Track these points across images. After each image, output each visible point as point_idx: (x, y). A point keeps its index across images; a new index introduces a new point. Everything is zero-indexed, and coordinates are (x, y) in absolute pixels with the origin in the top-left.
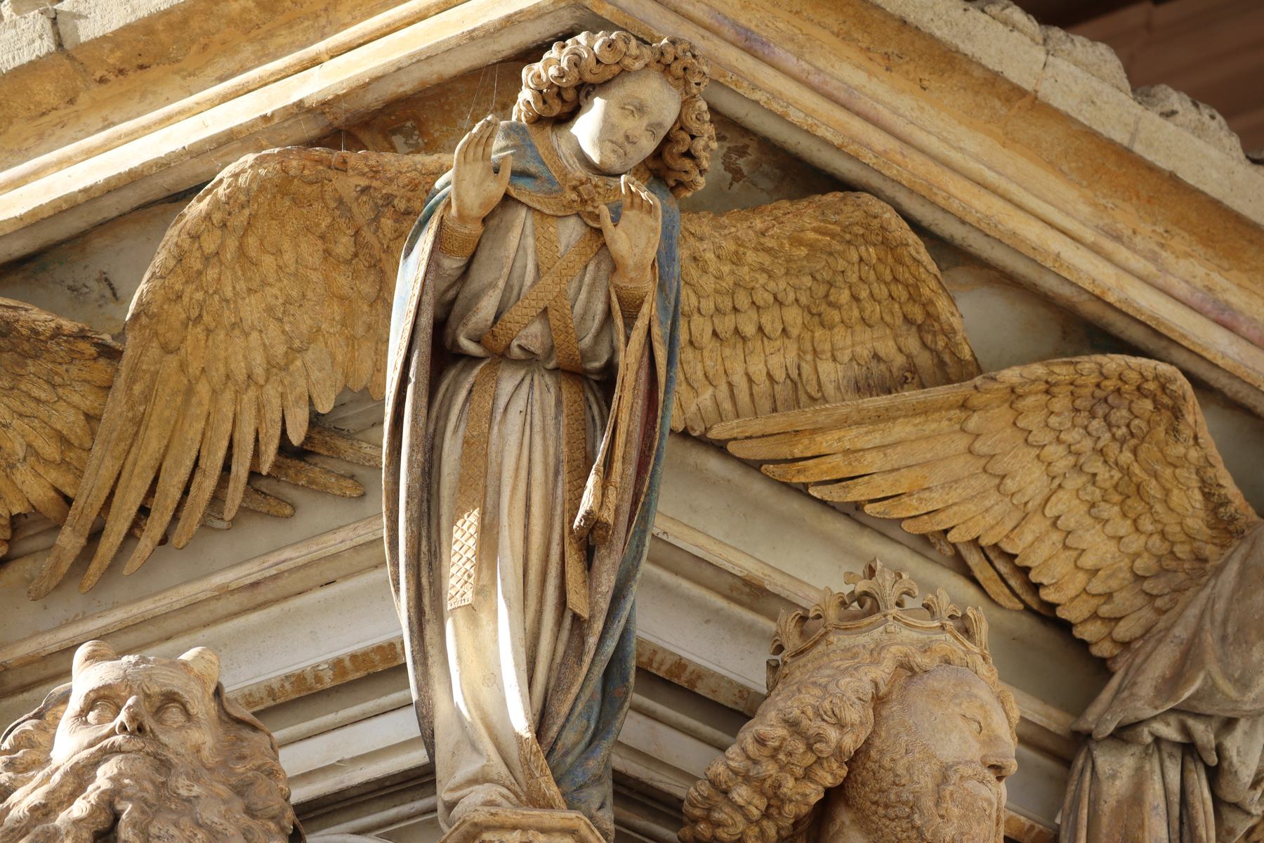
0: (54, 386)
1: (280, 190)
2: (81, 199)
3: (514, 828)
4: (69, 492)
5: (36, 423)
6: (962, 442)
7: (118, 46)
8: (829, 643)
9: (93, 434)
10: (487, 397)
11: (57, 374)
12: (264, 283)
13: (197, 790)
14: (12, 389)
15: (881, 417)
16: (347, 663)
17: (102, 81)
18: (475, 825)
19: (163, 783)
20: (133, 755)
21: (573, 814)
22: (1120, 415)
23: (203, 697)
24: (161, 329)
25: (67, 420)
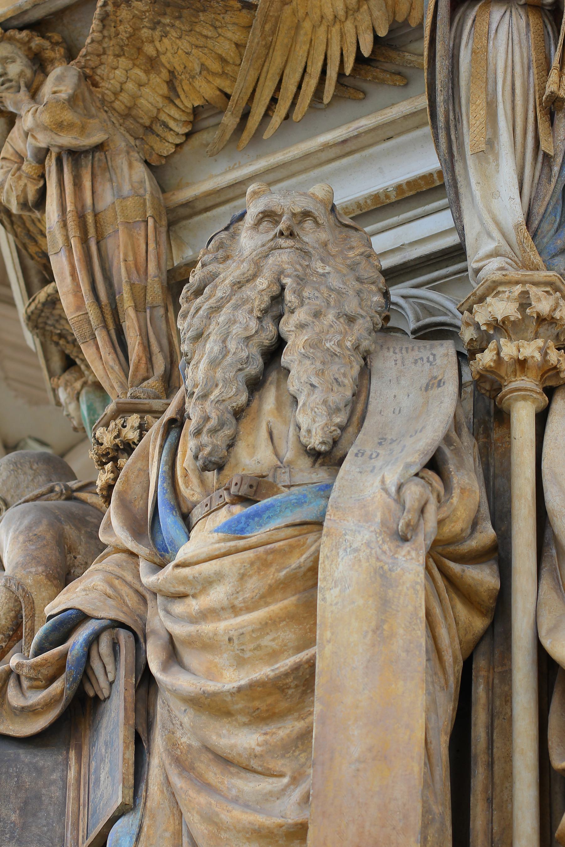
0: (216, 28)
3: (517, 283)
4: (228, 91)
5: (206, 51)
9: (241, 55)
10: (485, 24)
11: (217, 20)
13: (328, 269)
14: (191, 31)
16: (405, 187)
18: (494, 282)
19: (307, 266)
20: (288, 250)
21: (551, 273)
23: (325, 213)
25: (225, 48)
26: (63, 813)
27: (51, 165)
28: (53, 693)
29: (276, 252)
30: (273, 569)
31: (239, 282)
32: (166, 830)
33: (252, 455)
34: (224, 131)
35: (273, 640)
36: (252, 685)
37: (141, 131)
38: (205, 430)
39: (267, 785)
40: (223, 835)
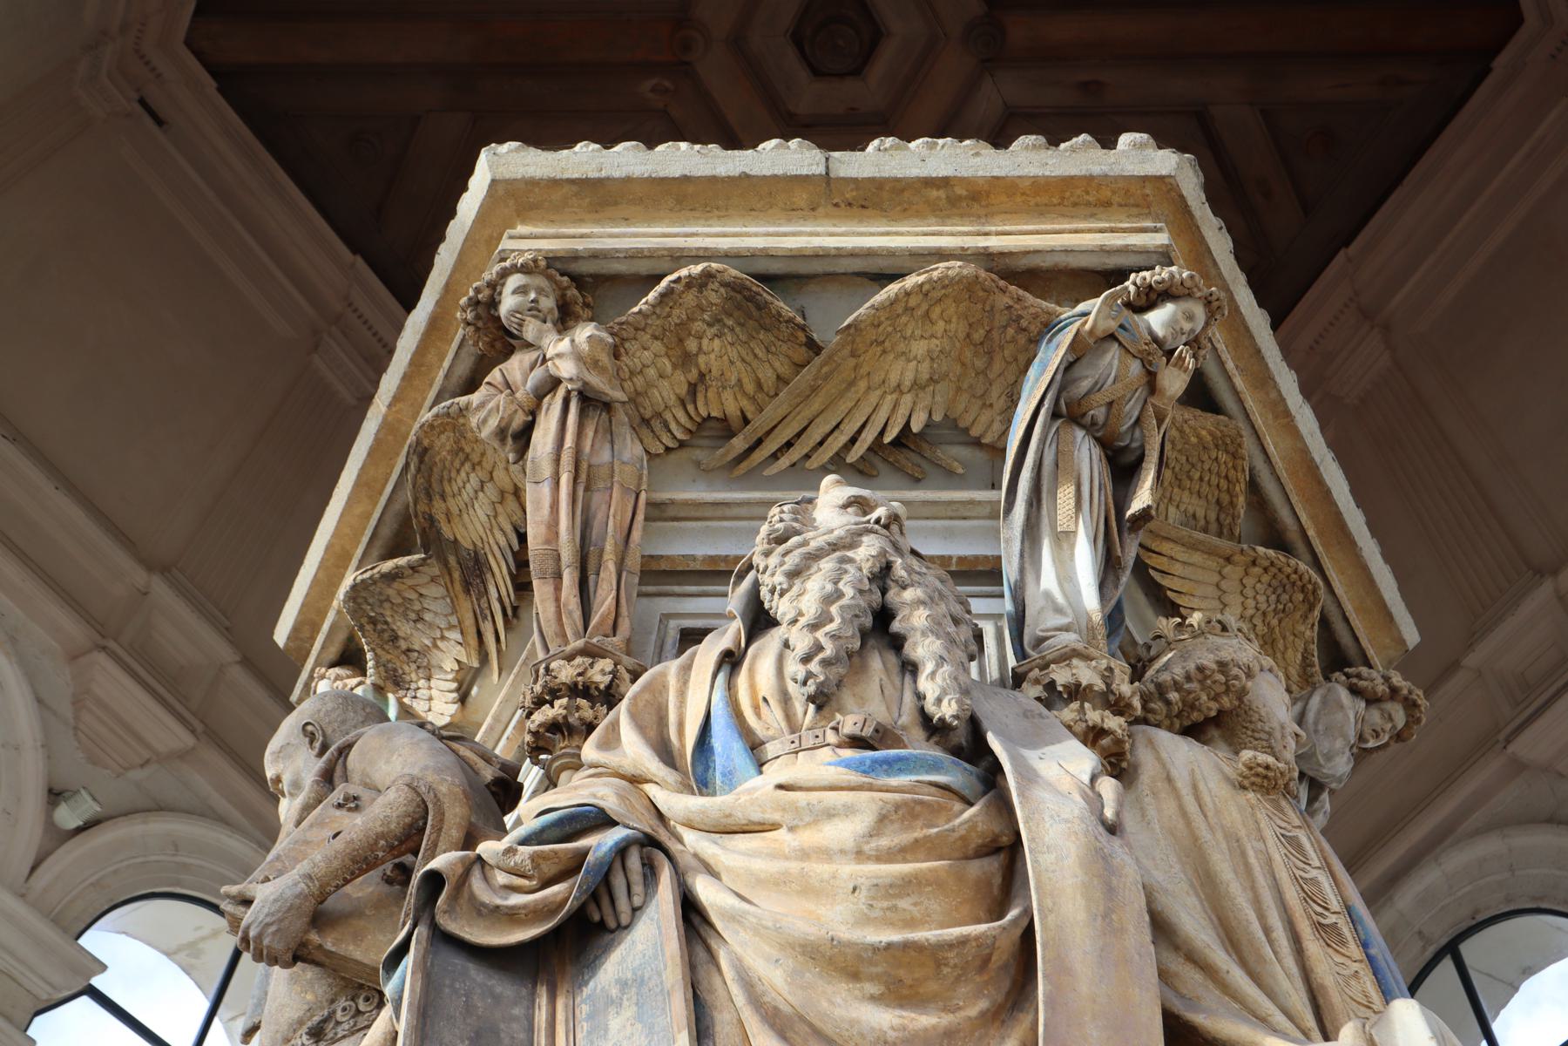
1: (969, 287)
2: (833, 252)
4: (749, 416)
6: (1216, 578)
7: (857, 189)
12: (932, 336)
15: (1193, 546)
17: (836, 205)
22: (1285, 597)
24: (858, 340)
25: (767, 376)
27: (553, 405)
34: (728, 452)
36: (906, 946)
37: (638, 420)
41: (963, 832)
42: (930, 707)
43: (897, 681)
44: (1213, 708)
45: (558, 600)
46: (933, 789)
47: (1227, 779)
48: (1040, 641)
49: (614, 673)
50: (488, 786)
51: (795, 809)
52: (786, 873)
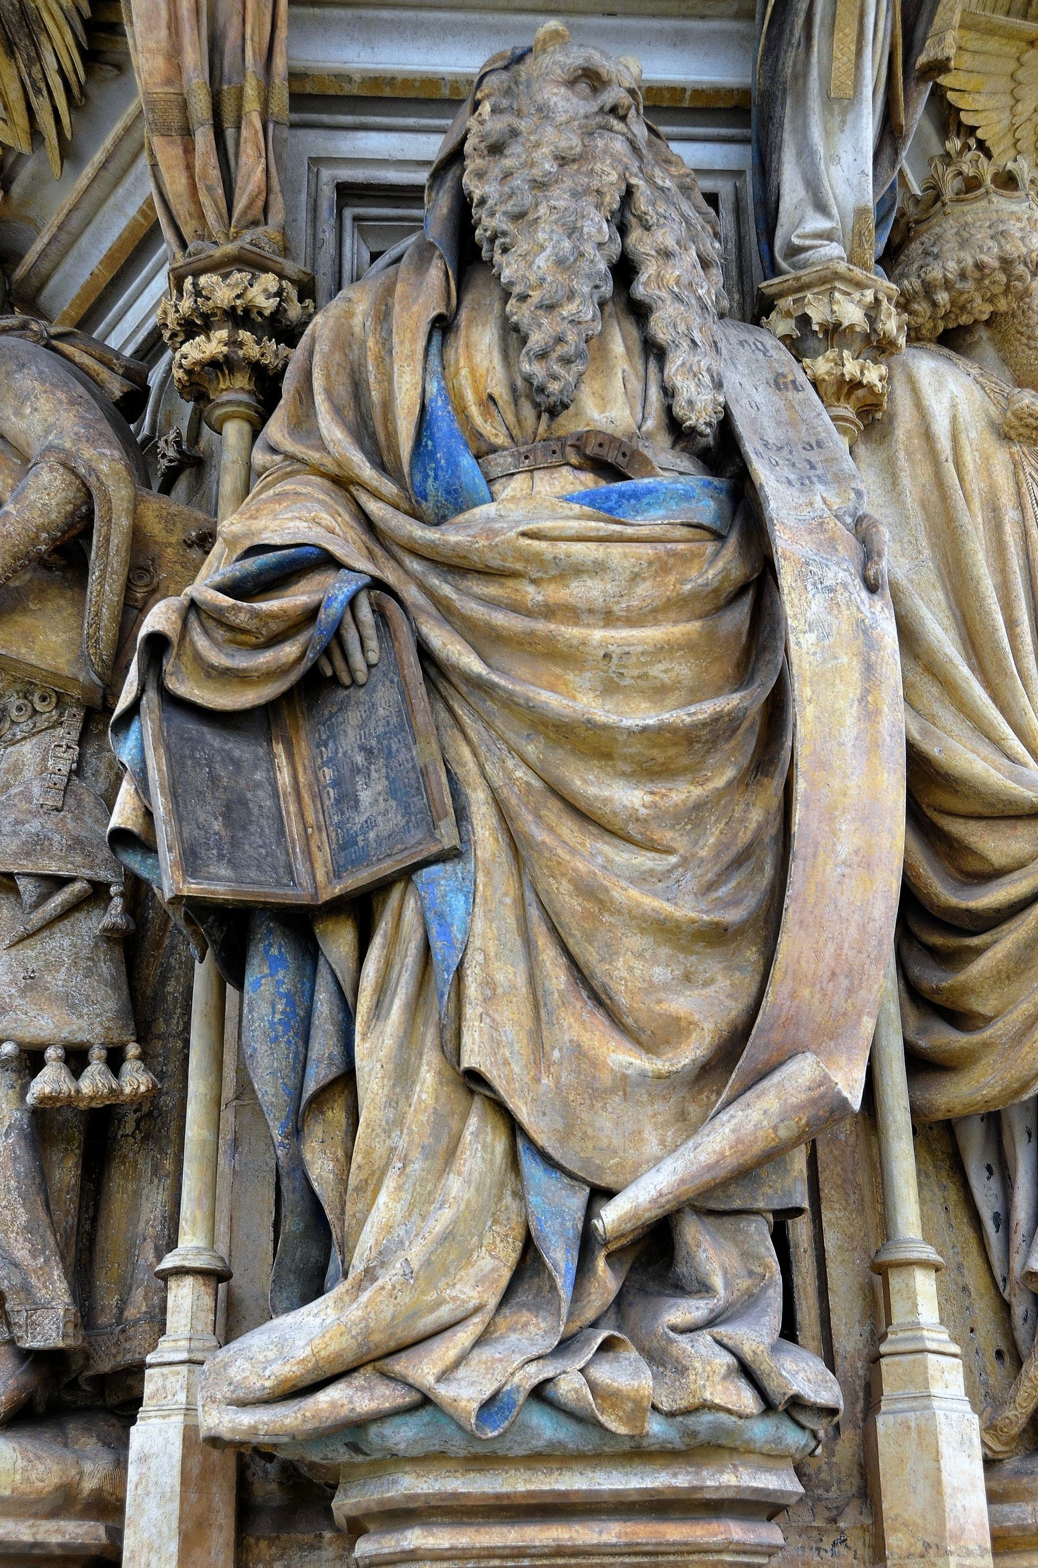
6: (1012, 65)
8: (990, 202)
15: (991, 31)
18: (836, 273)
26: (281, 832)
28: (284, 660)
29: (607, 134)
30: (672, 578)
31: (563, 158)
32: (506, 894)
33: (603, 409)
35: (666, 671)
36: (661, 729)
38: (554, 356)
39: (645, 860)
40: (606, 918)
41: (716, 584)
42: (678, 411)
43: (640, 368)
44: (983, 310)
45: (189, 167)
46: (685, 532)
47: (988, 416)
48: (793, 251)
49: (279, 293)
50: (116, 404)
51: (537, 559)
52: (532, 633)
